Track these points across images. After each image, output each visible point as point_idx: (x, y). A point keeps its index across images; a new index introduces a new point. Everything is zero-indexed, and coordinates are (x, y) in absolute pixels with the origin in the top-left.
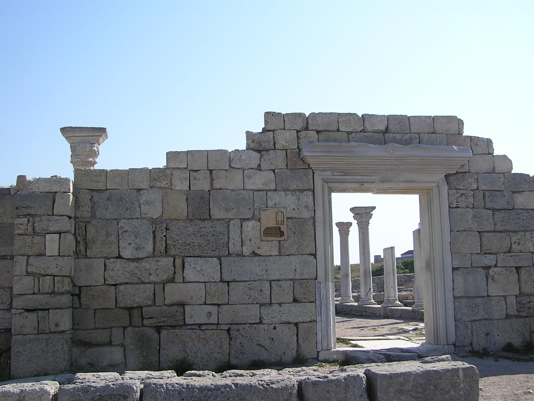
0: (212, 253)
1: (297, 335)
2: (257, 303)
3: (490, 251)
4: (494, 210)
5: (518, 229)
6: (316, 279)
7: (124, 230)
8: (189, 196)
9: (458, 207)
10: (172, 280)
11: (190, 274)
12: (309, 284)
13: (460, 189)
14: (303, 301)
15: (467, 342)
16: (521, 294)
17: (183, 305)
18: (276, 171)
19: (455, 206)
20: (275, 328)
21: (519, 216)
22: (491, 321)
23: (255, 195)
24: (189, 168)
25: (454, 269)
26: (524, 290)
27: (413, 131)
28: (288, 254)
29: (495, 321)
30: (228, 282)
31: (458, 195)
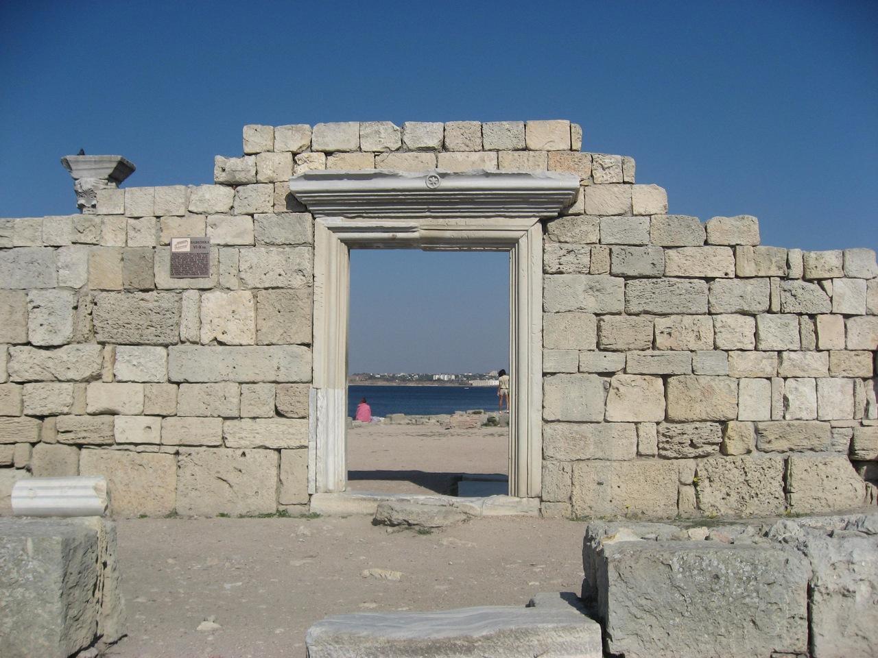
0: (155, 340)
2: (219, 416)
3: (614, 347)
4: (627, 278)
5: (670, 311)
7: (34, 304)
9: (561, 273)
10: (97, 377)
14: (289, 415)
15: (563, 495)
18: (255, 216)
19: (554, 270)
20: (244, 454)
21: (672, 288)
22: (608, 463)
24: (128, 214)
25: (544, 374)
26: (672, 414)
27: (486, 147)
28: (267, 343)
29: (615, 464)
31: (564, 252)
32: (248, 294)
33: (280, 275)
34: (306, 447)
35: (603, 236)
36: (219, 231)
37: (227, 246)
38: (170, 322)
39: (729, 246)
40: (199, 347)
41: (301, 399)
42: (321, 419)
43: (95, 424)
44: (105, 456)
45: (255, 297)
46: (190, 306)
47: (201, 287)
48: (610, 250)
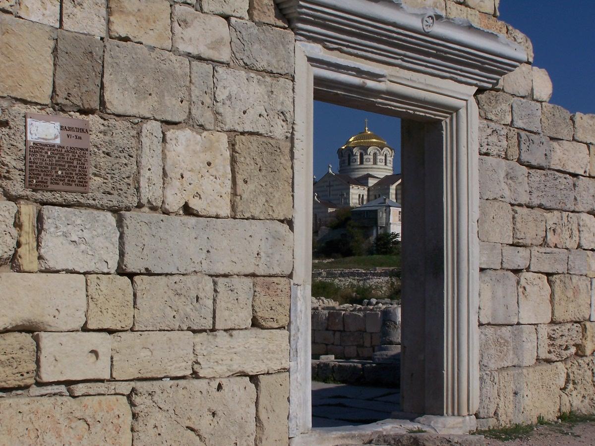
1: (257, 403)
5: (554, 207)
6: (290, 276)
8: (60, 46)
11: (56, 249)
12: (280, 287)
15: (492, 411)
16: (553, 322)
17: (31, 329)
18: (233, 20)
20: (220, 387)
23: (195, 68)
25: (482, 270)
29: (525, 371)
30: (131, 276)
32: (224, 138)
34: (288, 370)
35: (515, 118)
36: (189, 33)
37: (200, 58)
38: (127, 171)
39: (586, 143)
40: (159, 216)
43: (9, 350)
44: (25, 409)
45: (232, 145)
46: (154, 147)
47: (169, 118)
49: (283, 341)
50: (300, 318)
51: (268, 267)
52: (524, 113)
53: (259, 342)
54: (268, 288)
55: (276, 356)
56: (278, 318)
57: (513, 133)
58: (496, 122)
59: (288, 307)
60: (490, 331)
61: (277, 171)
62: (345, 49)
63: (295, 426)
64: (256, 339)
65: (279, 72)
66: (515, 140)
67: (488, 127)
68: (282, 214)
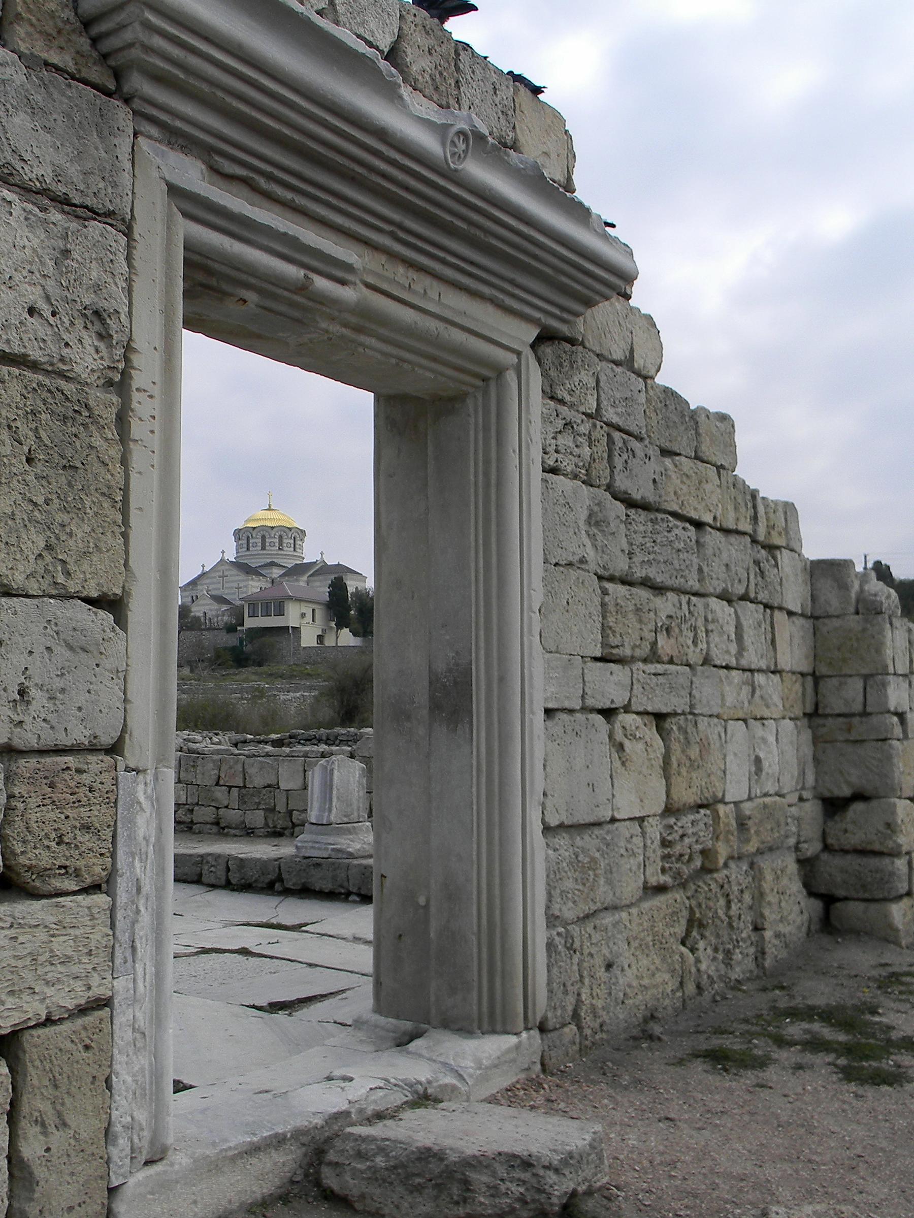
5: (669, 582)
6: (115, 749)
12: (86, 778)
13: (561, 402)
16: (669, 810)
25: (549, 712)
33: (32, 311)
41: (98, 815)
42: (147, 888)
48: (611, 441)
49: (93, 927)
50: (144, 857)
51: (52, 728)
52: (618, 395)
53: (21, 939)
54: (52, 786)
55: (75, 969)
56: (81, 864)
57: (600, 433)
58: (572, 406)
59: (107, 834)
60: (562, 840)
61: (79, 465)
62: (262, 182)
63: (128, 1150)
64: (11, 933)
65: (88, 202)
66: (601, 448)
67: (557, 416)
68: (92, 583)
